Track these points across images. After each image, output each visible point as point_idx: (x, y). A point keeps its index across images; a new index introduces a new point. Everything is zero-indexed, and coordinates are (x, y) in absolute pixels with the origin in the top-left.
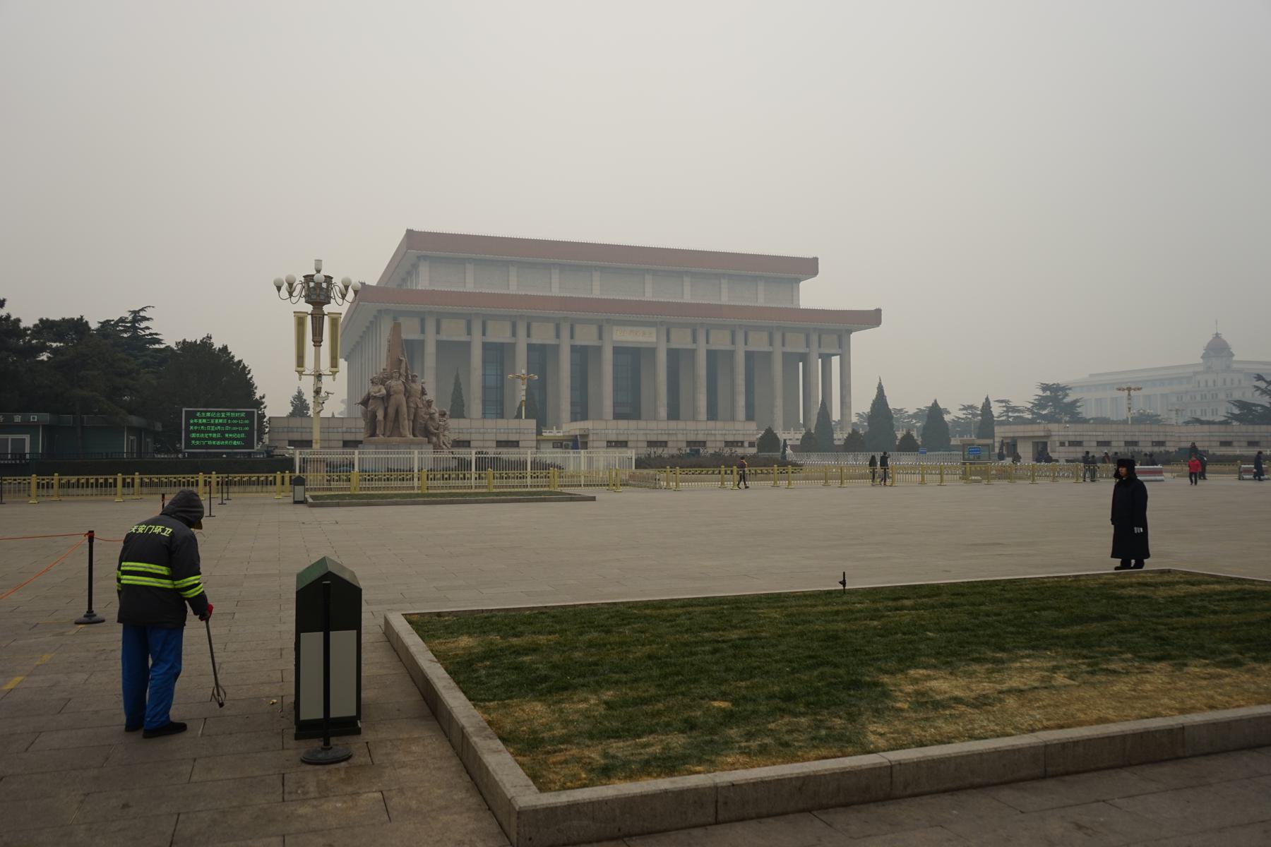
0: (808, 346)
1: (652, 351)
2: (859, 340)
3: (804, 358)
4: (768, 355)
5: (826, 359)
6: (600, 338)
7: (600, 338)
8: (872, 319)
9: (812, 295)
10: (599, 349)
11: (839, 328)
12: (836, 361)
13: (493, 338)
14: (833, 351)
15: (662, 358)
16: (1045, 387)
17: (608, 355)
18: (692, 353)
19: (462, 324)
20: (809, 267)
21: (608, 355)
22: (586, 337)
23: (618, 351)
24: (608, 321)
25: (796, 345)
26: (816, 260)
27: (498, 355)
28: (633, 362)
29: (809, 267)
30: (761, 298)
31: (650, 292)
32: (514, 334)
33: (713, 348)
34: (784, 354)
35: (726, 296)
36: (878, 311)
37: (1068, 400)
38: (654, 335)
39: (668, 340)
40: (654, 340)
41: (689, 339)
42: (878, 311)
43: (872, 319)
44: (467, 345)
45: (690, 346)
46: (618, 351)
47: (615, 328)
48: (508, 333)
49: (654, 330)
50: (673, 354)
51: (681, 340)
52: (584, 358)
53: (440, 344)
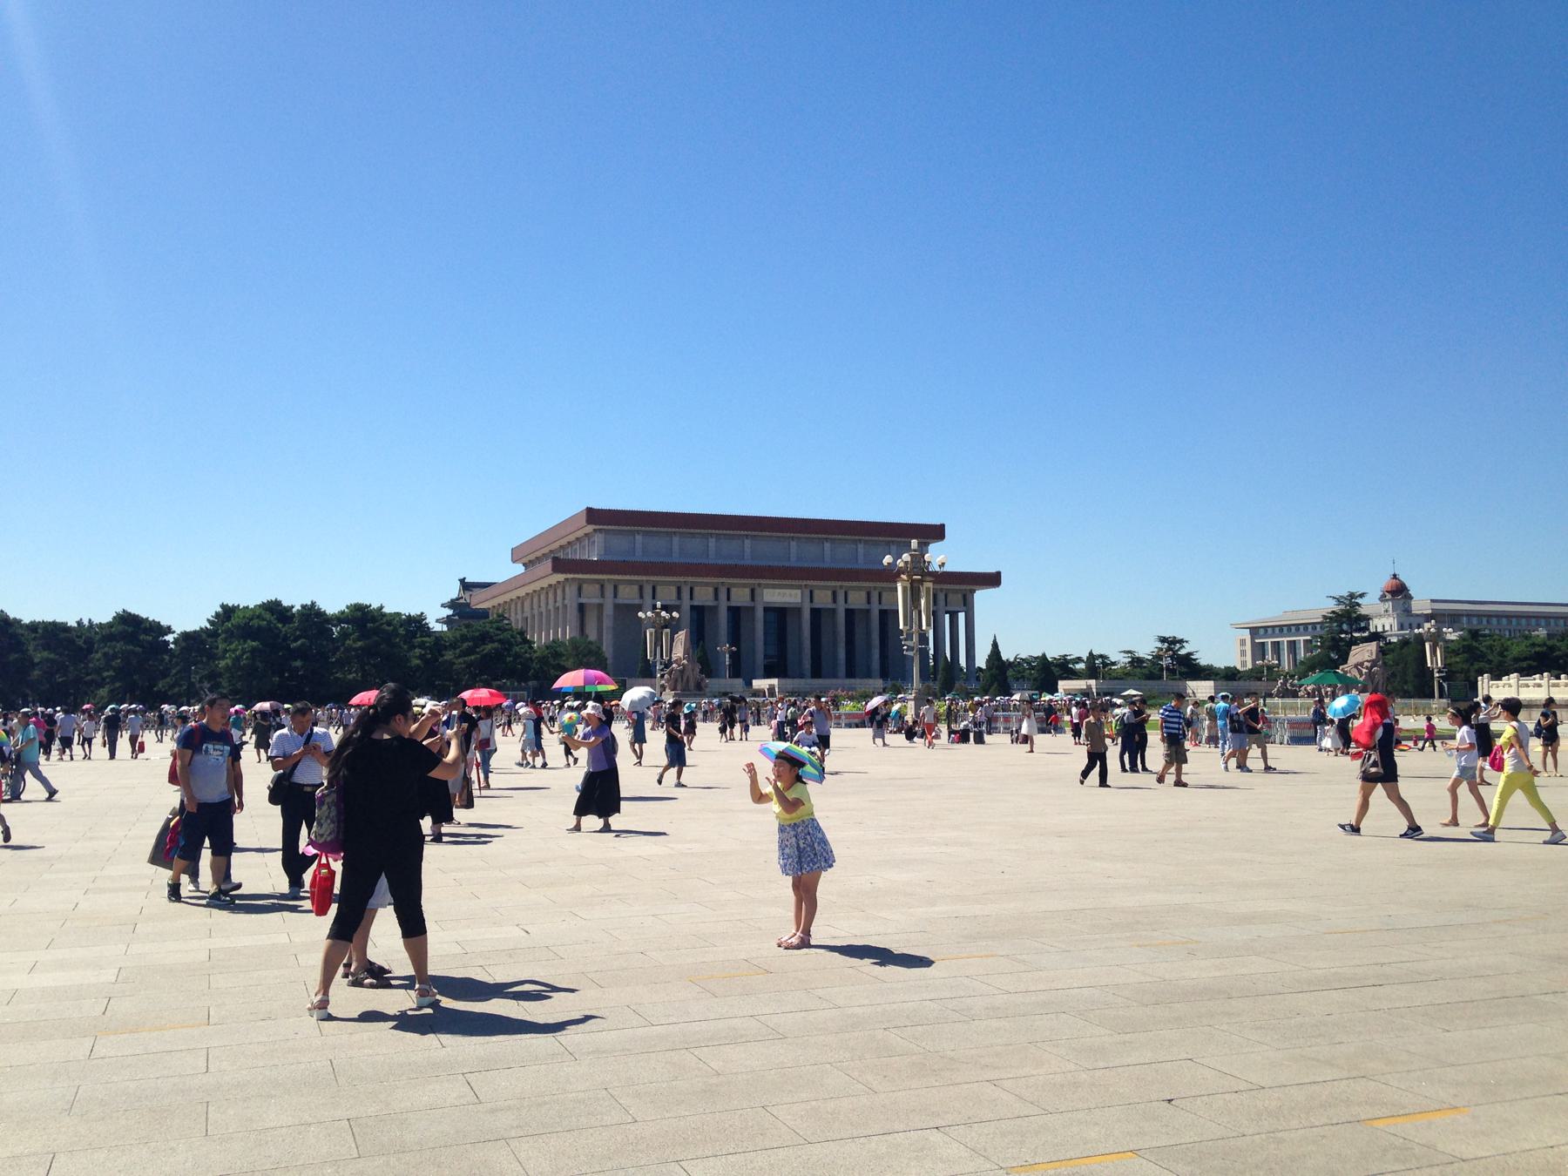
1: (797, 610)
2: (982, 597)
6: (753, 599)
7: (753, 599)
8: (993, 580)
9: (939, 556)
10: (752, 609)
11: (962, 588)
12: (962, 616)
15: (806, 615)
16: (1163, 640)
17: (760, 614)
20: (937, 532)
22: (740, 597)
23: (766, 610)
26: (943, 526)
28: (780, 616)
29: (936, 533)
36: (999, 574)
37: (1182, 652)
42: (999, 574)
43: (993, 580)
46: (766, 610)
50: (816, 613)
53: (617, 607)
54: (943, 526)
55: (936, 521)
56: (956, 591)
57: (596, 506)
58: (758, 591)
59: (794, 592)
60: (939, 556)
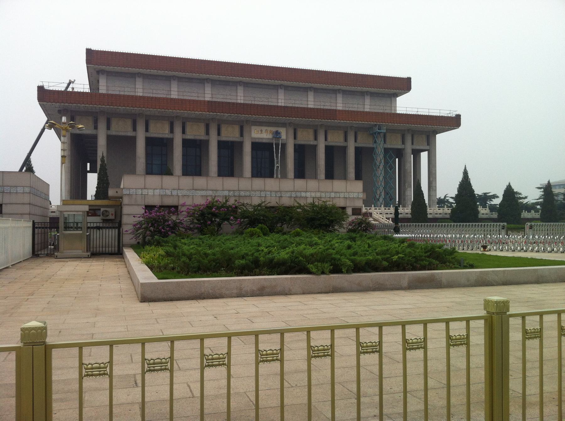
0: (403, 143)
2: (443, 140)
3: (399, 153)
4: (371, 151)
5: (416, 154)
6: (242, 135)
7: (242, 135)
8: (454, 122)
9: (405, 104)
10: (240, 145)
12: (424, 156)
14: (422, 148)
15: (290, 151)
17: (247, 149)
18: (314, 148)
19: (129, 123)
21: (247, 149)
22: (230, 134)
24: (247, 121)
25: (395, 143)
30: (368, 106)
31: (281, 100)
32: (172, 131)
33: (331, 144)
34: (386, 150)
35: (340, 104)
36: (458, 117)
39: (295, 138)
41: (312, 137)
42: (458, 117)
43: (454, 122)
45: (313, 142)
47: (253, 128)
48: (167, 130)
51: (306, 137)
54: (409, 80)
55: (404, 75)
56: (421, 132)
58: (246, 129)
60: (405, 104)
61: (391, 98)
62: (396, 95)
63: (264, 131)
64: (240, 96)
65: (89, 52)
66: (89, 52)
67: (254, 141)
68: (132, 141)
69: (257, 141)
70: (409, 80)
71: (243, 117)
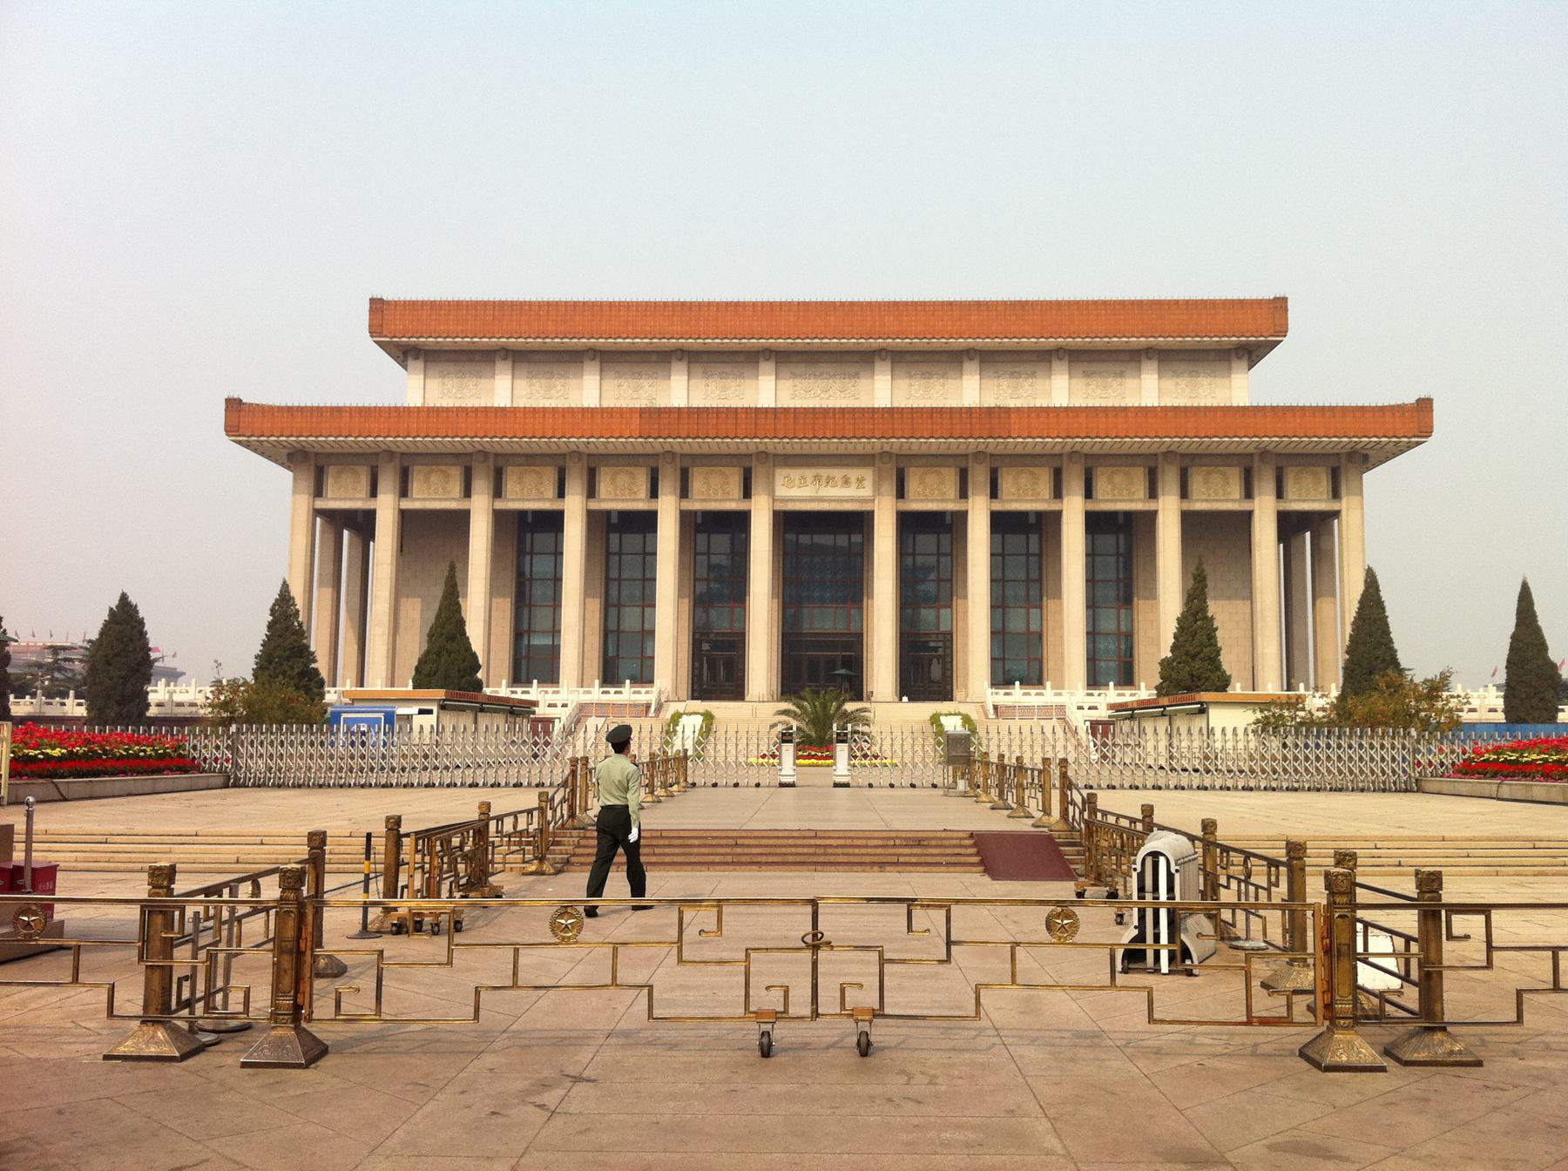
7: (747, 494)
13: (1013, 502)
19: (456, 473)
23: (789, 523)
27: (528, 534)
30: (1148, 389)
31: (882, 390)
36: (1425, 405)
38: (868, 483)
39: (901, 494)
40: (866, 492)
42: (1425, 405)
44: (463, 518)
47: (781, 474)
49: (868, 474)
52: (716, 534)
53: (405, 517)
54: (1280, 304)
56: (1306, 459)
57: (390, 295)
59: (853, 473)
61: (1229, 360)
62: (1252, 353)
63: (809, 480)
64: (765, 390)
65: (377, 305)
66: (377, 305)
67: (780, 507)
68: (460, 521)
69: (791, 507)
70: (1280, 304)
71: (751, 444)
